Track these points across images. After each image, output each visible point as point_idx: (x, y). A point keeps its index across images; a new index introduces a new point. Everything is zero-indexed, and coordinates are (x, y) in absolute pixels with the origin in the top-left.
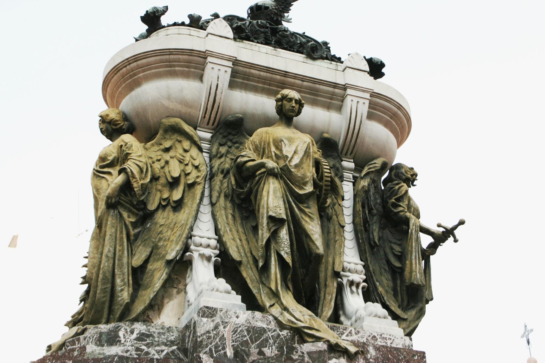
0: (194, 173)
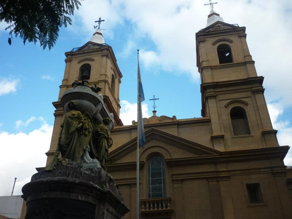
0: (90, 129)
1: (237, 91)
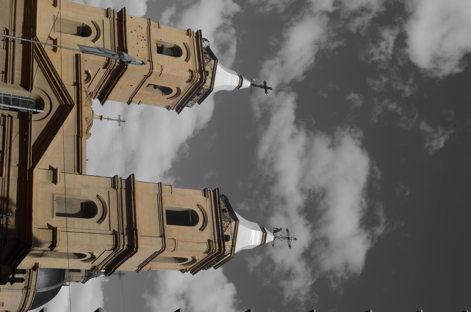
1: (120, 215)
